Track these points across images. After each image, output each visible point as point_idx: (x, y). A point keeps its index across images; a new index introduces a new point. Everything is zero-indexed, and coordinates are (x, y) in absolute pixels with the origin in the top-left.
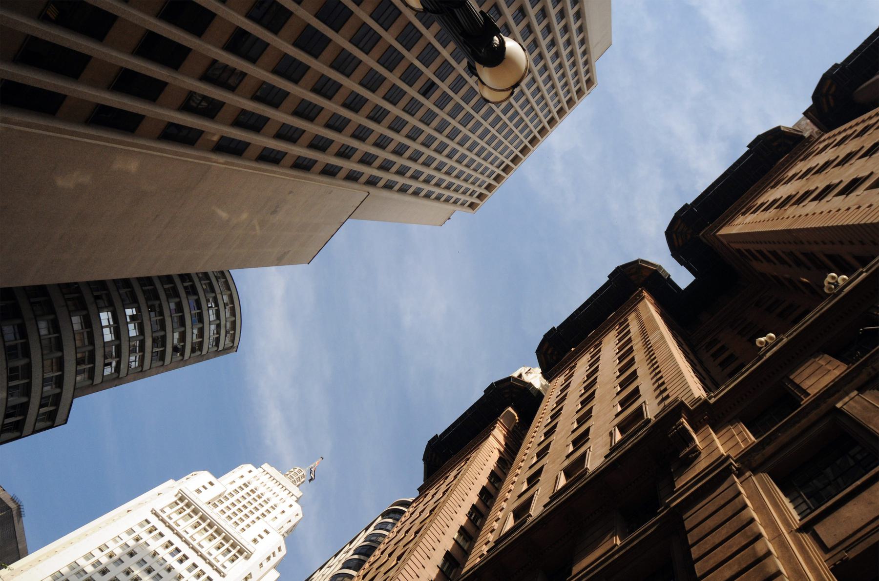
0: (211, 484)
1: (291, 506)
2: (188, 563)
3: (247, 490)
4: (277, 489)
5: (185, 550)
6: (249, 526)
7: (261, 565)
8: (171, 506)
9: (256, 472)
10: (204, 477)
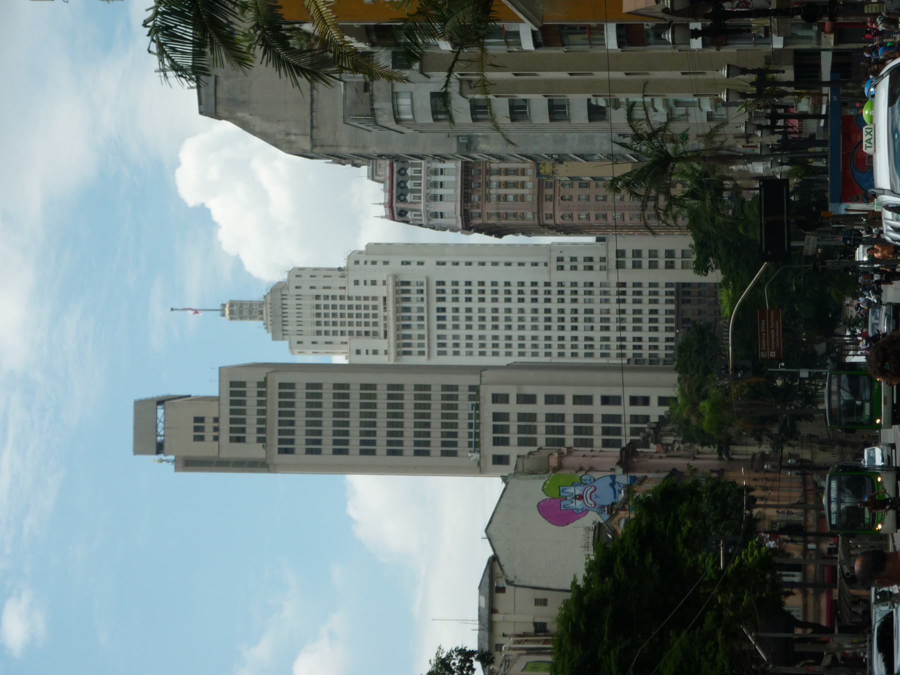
1: (297, 287)
2: (441, 305)
3: (323, 328)
4: (291, 311)
5: (434, 314)
6: (358, 298)
7: (386, 263)
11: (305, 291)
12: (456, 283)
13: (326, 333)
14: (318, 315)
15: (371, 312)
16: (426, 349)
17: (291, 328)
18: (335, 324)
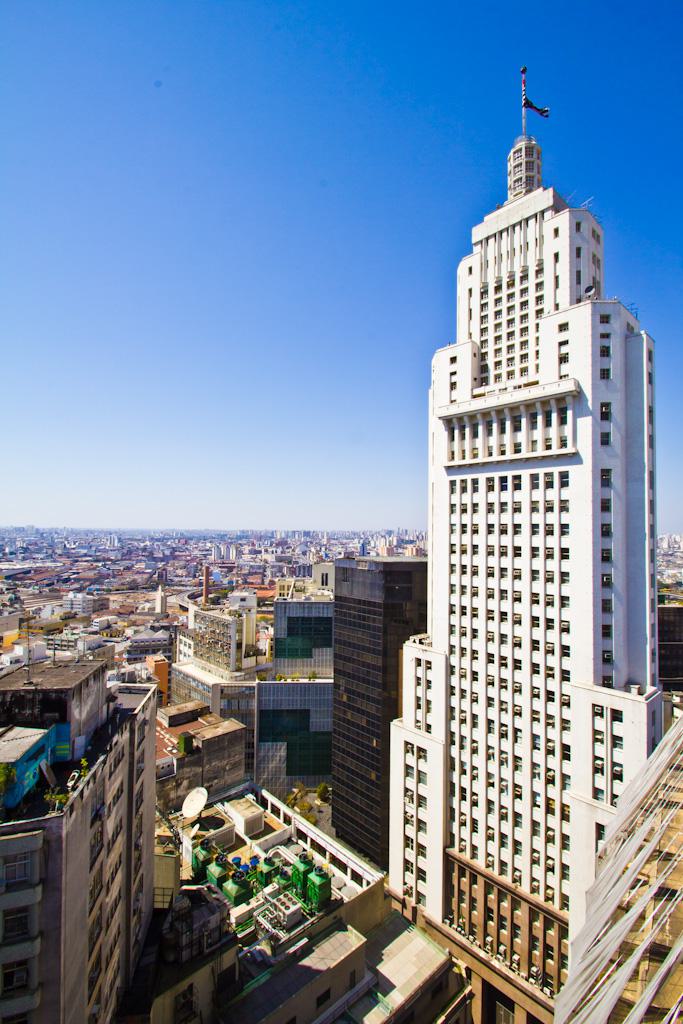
1: (556, 231)
2: (526, 482)
3: (491, 297)
7: (605, 374)
9: (473, 260)
10: (440, 360)
11: (552, 245)
12: (564, 507)
15: (517, 366)
16: (457, 462)
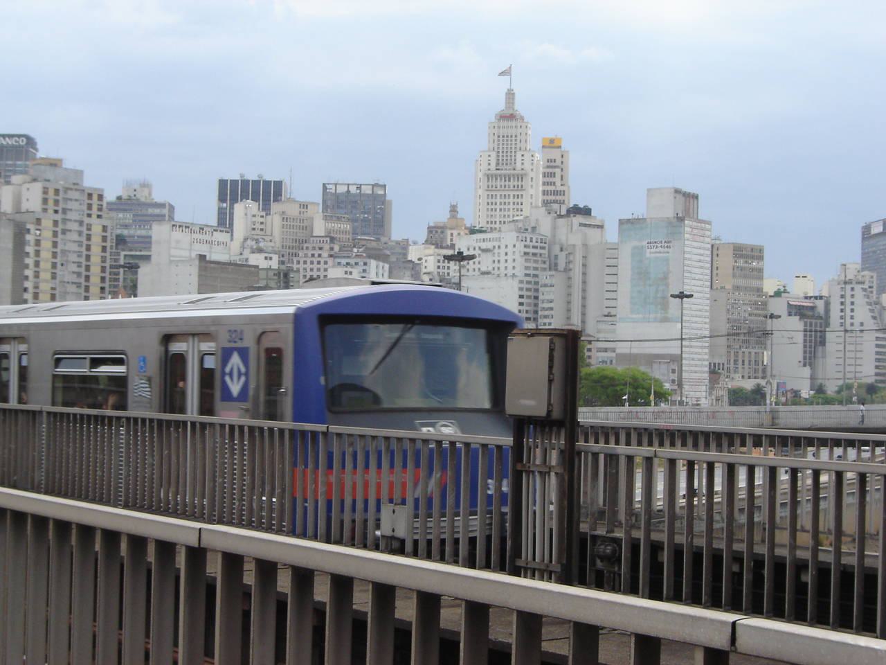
0: (489, 156)
3: (501, 138)
4: (510, 123)
5: (507, 193)
7: (532, 170)
8: (488, 181)
13: (499, 141)
14: (507, 136)
16: (490, 189)
17: (502, 124)
18: (503, 144)
